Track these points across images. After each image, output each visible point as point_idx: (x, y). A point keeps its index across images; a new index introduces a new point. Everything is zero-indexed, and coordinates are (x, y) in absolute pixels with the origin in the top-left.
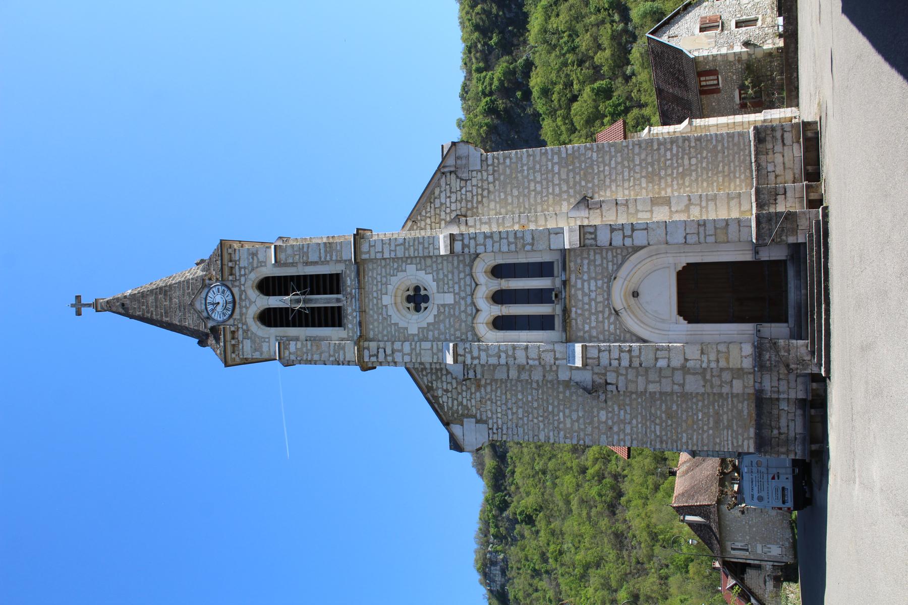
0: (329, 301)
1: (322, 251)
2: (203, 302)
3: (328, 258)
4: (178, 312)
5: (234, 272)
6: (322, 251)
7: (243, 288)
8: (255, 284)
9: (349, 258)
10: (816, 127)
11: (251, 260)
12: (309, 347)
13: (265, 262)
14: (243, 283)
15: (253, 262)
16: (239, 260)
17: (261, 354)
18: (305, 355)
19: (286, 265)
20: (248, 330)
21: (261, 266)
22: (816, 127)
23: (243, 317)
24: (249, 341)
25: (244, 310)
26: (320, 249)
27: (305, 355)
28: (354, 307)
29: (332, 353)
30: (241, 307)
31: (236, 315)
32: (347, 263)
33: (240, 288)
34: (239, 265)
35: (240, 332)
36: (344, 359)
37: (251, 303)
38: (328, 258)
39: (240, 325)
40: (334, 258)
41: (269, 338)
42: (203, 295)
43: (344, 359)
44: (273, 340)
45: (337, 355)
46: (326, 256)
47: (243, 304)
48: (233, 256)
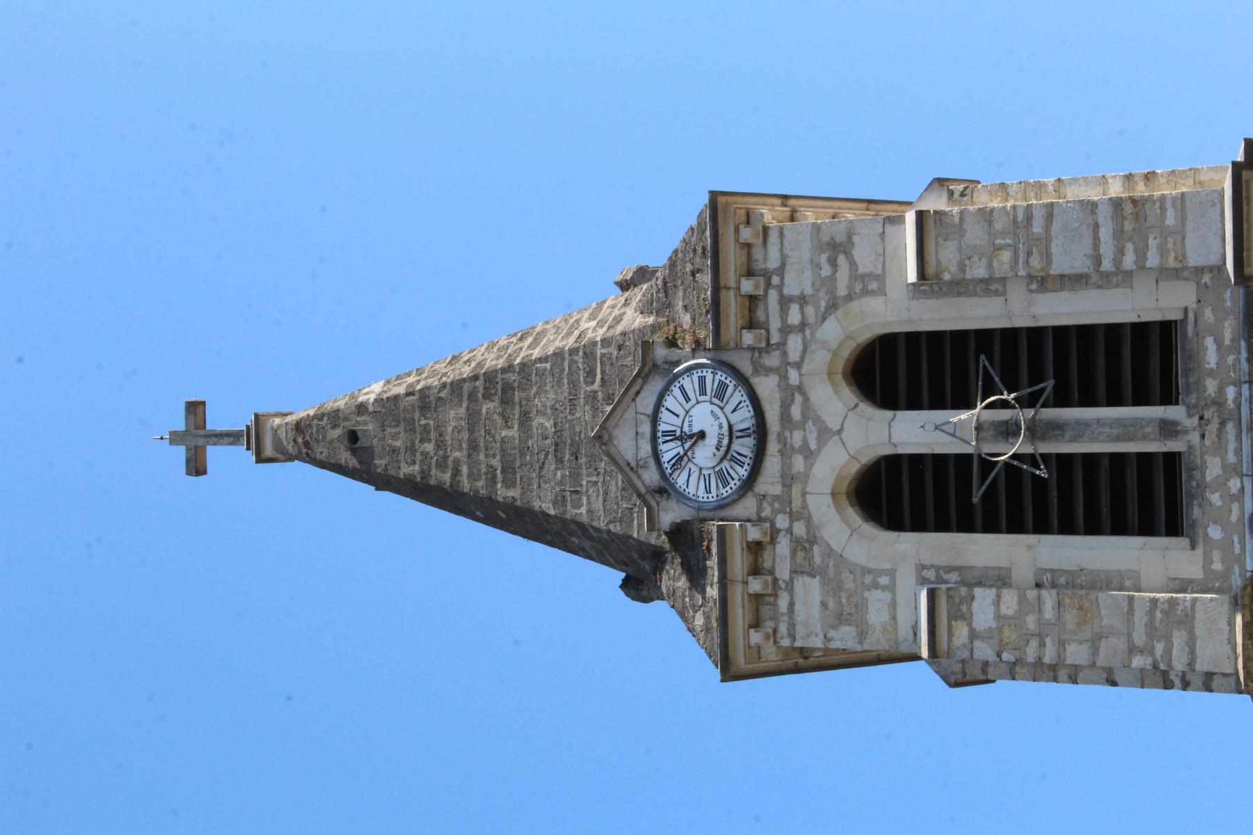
0: (1129, 430)
1: (1105, 234)
2: (646, 428)
3: (1129, 261)
4: (551, 466)
5: (760, 314)
6: (1105, 234)
7: (794, 377)
8: (840, 365)
9: (1213, 260)
10: (1120, 597)
11: (826, 271)
12: (1049, 614)
13: (881, 278)
14: (794, 355)
15: (832, 278)
16: (781, 270)
17: (862, 635)
18: (1034, 643)
19: (960, 287)
20: (812, 540)
21: (866, 292)
22: (1120, 597)
23: (796, 491)
24: (816, 582)
25: (798, 463)
26: (1096, 227)
27: (1034, 643)
28: (1231, 458)
29: (1139, 637)
30: (786, 452)
31: (769, 483)
32: (1206, 279)
33: (784, 377)
34: (780, 288)
35: (783, 546)
36: (1191, 664)
37: (825, 433)
38: (1129, 261)
39: (782, 522)
40: (1153, 260)
41: (892, 573)
42: (646, 402)
43: (1191, 664)
44: (906, 579)
45: (1159, 647)
46: (1121, 251)
47: (796, 438)
48: (758, 253)
